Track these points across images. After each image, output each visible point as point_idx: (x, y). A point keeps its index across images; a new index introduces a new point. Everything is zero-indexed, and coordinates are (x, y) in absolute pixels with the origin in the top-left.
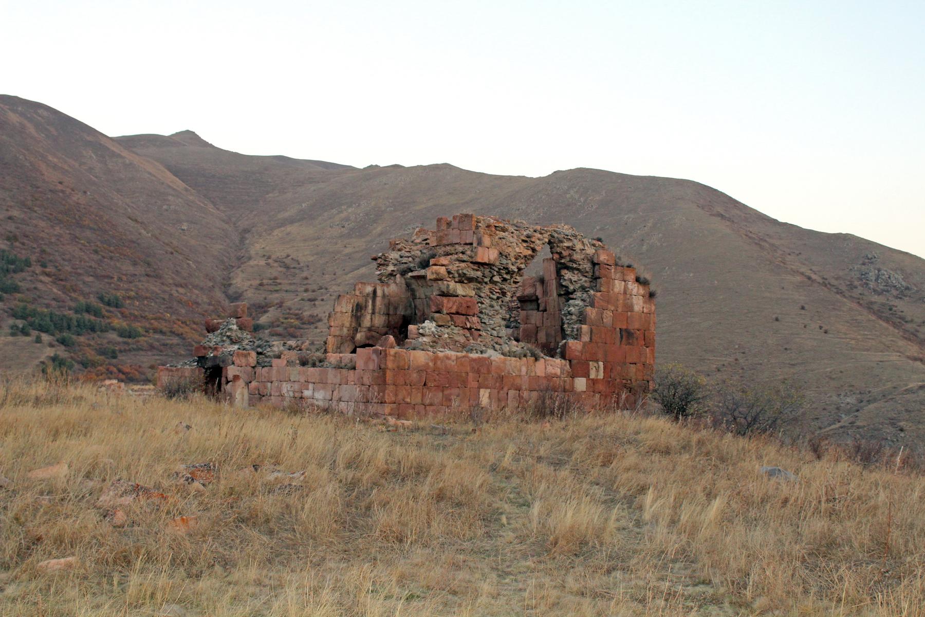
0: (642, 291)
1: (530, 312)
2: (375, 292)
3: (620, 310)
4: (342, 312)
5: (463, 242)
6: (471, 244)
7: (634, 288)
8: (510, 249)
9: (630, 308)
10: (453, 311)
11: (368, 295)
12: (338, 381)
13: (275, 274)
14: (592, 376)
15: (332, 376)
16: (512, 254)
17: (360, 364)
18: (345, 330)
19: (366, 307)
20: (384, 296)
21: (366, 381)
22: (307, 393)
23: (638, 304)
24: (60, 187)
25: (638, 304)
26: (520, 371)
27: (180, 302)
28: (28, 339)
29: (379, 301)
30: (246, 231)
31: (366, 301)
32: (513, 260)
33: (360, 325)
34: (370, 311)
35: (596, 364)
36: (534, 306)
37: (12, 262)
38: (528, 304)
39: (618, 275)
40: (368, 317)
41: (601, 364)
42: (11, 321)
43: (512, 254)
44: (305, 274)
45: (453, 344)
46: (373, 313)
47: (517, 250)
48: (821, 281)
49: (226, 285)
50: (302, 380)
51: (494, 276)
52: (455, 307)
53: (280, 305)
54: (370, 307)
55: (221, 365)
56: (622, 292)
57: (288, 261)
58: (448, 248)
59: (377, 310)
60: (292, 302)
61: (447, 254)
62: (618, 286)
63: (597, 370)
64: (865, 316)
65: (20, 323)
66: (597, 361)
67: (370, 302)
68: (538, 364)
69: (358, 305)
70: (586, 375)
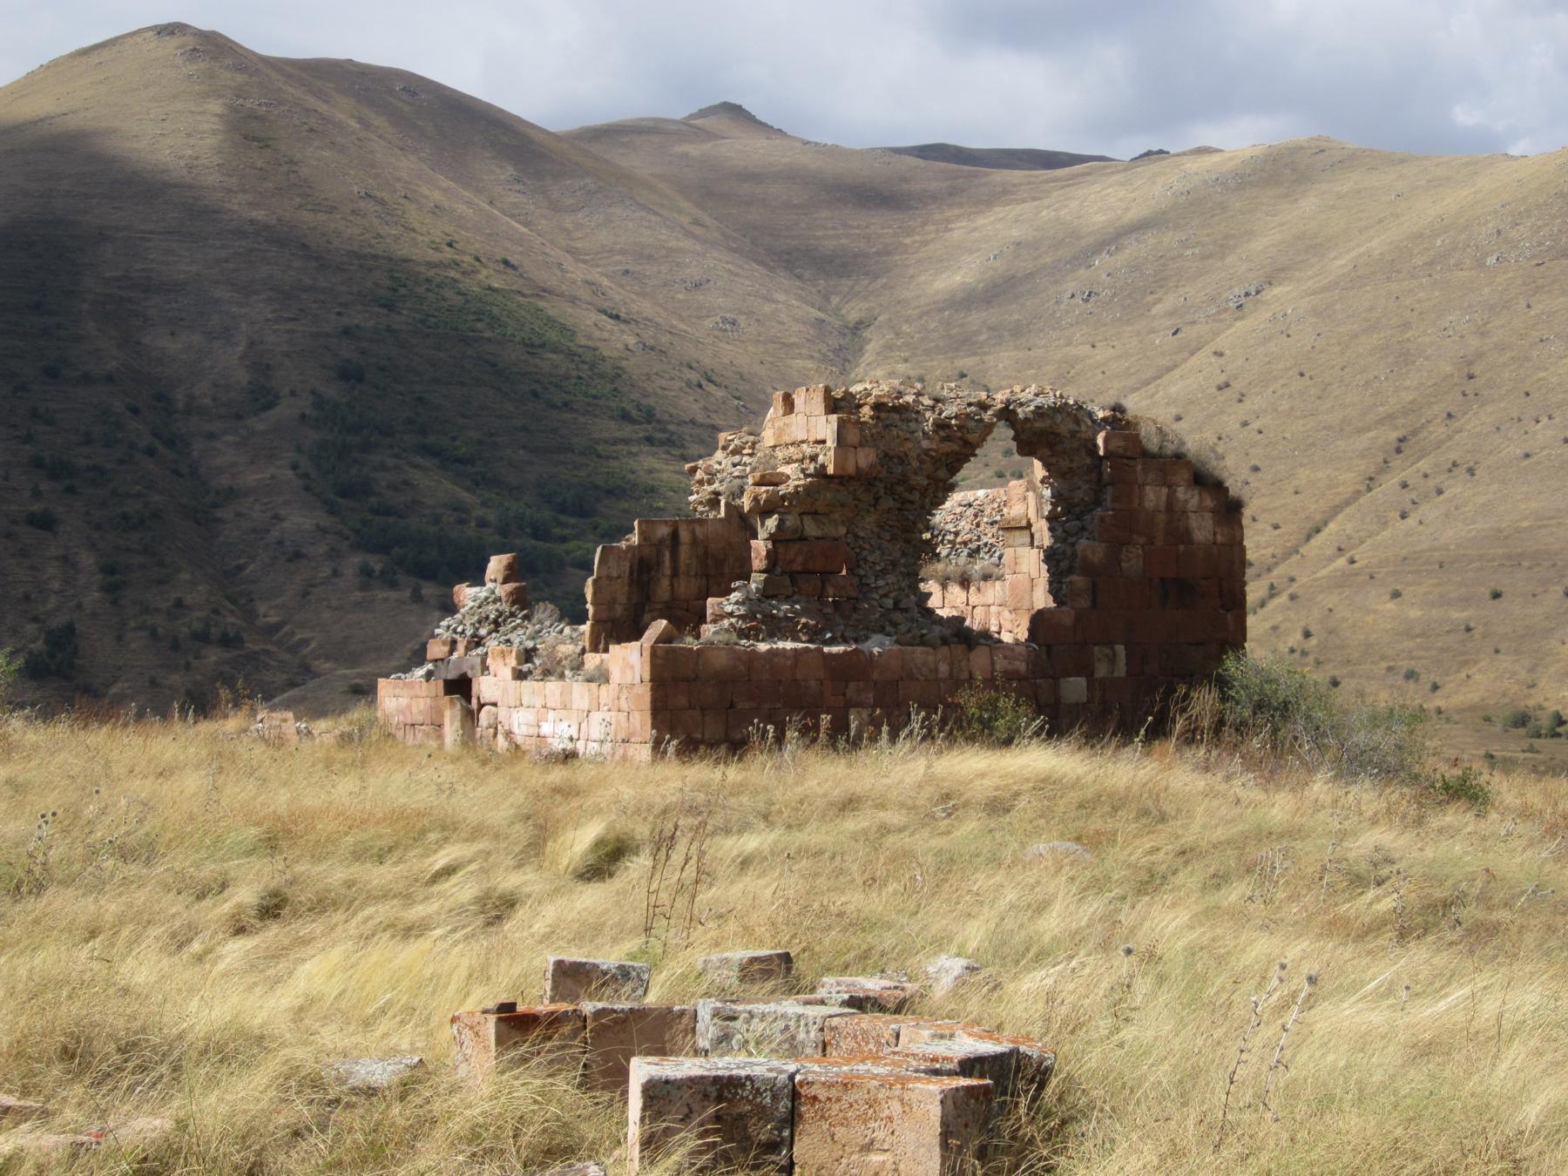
0: (1209, 503)
1: (1020, 550)
2: (675, 535)
3: (1159, 542)
4: (609, 578)
5: (812, 439)
6: (824, 442)
7: (1188, 497)
8: (909, 445)
9: (1185, 536)
10: (797, 567)
11: (661, 541)
12: (585, 705)
14: (1101, 671)
15: (579, 692)
16: (914, 454)
17: (616, 676)
18: (619, 609)
19: (659, 563)
20: (695, 541)
21: (624, 705)
22: (546, 729)
24: (448, 254)
26: (936, 670)
28: (394, 595)
29: (684, 552)
31: (659, 554)
32: (915, 464)
33: (648, 598)
34: (668, 572)
35: (1107, 651)
36: (1024, 537)
38: (1017, 533)
39: (1151, 476)
40: (665, 583)
41: (1120, 649)
42: (356, 559)
43: (914, 454)
46: (675, 574)
47: (925, 444)
50: (539, 702)
51: (877, 499)
52: (800, 559)
54: (667, 563)
55: (470, 674)
56: (1162, 508)
58: (792, 449)
59: (682, 568)
61: (789, 461)
62: (1153, 497)
63: (1112, 660)
65: (376, 563)
66: (1110, 644)
67: (667, 554)
68: (973, 655)
69: (641, 560)
70: (1086, 670)
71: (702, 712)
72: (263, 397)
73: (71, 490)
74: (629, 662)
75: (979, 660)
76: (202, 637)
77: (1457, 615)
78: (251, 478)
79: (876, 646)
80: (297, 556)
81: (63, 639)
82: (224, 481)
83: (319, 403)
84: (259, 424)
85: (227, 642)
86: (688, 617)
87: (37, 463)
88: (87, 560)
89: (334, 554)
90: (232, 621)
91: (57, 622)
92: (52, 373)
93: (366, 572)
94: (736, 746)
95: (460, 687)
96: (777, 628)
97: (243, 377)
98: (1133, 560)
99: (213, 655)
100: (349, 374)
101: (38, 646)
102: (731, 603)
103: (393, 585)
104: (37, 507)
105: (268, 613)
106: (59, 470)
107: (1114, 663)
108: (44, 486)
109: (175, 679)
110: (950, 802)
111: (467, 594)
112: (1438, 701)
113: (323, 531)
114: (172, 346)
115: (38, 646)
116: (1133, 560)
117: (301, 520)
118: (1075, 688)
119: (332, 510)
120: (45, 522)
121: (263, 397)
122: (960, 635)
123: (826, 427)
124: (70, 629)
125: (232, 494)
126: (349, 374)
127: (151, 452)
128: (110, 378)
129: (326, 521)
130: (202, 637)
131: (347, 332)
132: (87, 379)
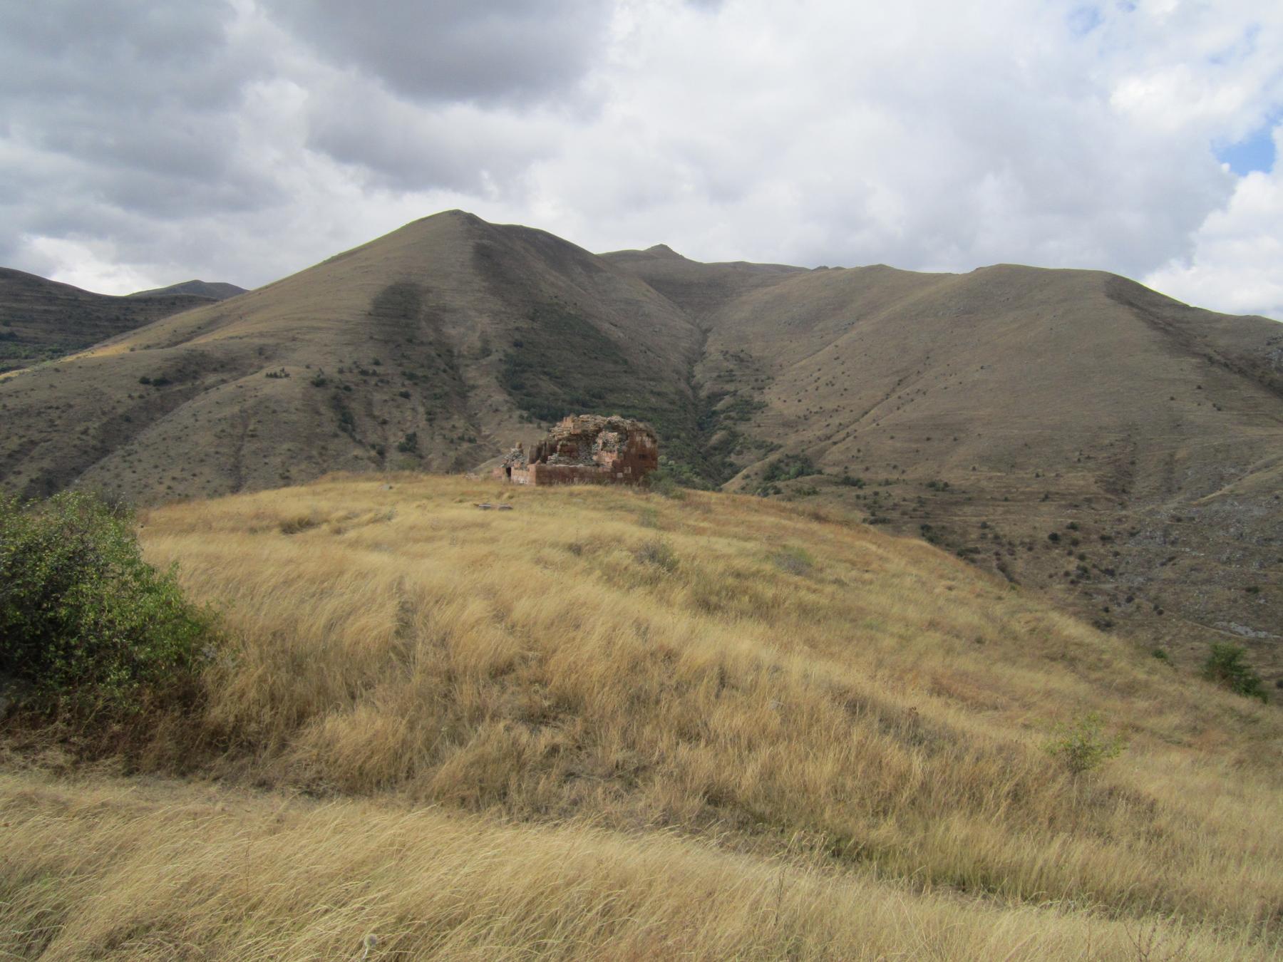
7: (646, 439)
13: (731, 367)
23: (649, 444)
24: (555, 301)
25: (649, 444)
27: (652, 392)
37: (519, 365)
42: (518, 413)
44: (757, 366)
45: (564, 462)
48: (1223, 361)
49: (691, 376)
53: (734, 393)
57: (742, 355)
60: (745, 390)
62: (638, 439)
64: (1260, 395)
65: (525, 414)
71: (545, 478)
72: (486, 352)
73: (416, 384)
74: (532, 467)
75: (600, 470)
76: (461, 439)
77: (914, 446)
78: (481, 382)
79: (581, 465)
80: (497, 410)
81: (412, 438)
82: (471, 382)
83: (506, 355)
84: (484, 362)
85: (470, 441)
86: (544, 460)
87: (404, 374)
88: (421, 410)
89: (510, 410)
90: (472, 433)
91: (410, 431)
92: (410, 341)
93: (521, 417)
94: (551, 484)
95: (509, 471)
96: (560, 462)
97: (479, 344)
99: (465, 445)
100: (517, 344)
101: (403, 440)
104: (403, 390)
105: (486, 431)
106: (411, 377)
108: (407, 382)
109: (452, 454)
110: (571, 494)
112: (904, 477)
113: (507, 402)
114: (453, 332)
115: (403, 440)
116: (633, 450)
117: (499, 397)
118: (620, 475)
119: (510, 394)
120: (406, 396)
121: (486, 352)
123: (571, 425)
124: (415, 435)
125: (473, 387)
126: (517, 344)
127: (445, 371)
128: (430, 343)
129: (508, 398)
130: (461, 439)
131: (517, 329)
132: (422, 343)
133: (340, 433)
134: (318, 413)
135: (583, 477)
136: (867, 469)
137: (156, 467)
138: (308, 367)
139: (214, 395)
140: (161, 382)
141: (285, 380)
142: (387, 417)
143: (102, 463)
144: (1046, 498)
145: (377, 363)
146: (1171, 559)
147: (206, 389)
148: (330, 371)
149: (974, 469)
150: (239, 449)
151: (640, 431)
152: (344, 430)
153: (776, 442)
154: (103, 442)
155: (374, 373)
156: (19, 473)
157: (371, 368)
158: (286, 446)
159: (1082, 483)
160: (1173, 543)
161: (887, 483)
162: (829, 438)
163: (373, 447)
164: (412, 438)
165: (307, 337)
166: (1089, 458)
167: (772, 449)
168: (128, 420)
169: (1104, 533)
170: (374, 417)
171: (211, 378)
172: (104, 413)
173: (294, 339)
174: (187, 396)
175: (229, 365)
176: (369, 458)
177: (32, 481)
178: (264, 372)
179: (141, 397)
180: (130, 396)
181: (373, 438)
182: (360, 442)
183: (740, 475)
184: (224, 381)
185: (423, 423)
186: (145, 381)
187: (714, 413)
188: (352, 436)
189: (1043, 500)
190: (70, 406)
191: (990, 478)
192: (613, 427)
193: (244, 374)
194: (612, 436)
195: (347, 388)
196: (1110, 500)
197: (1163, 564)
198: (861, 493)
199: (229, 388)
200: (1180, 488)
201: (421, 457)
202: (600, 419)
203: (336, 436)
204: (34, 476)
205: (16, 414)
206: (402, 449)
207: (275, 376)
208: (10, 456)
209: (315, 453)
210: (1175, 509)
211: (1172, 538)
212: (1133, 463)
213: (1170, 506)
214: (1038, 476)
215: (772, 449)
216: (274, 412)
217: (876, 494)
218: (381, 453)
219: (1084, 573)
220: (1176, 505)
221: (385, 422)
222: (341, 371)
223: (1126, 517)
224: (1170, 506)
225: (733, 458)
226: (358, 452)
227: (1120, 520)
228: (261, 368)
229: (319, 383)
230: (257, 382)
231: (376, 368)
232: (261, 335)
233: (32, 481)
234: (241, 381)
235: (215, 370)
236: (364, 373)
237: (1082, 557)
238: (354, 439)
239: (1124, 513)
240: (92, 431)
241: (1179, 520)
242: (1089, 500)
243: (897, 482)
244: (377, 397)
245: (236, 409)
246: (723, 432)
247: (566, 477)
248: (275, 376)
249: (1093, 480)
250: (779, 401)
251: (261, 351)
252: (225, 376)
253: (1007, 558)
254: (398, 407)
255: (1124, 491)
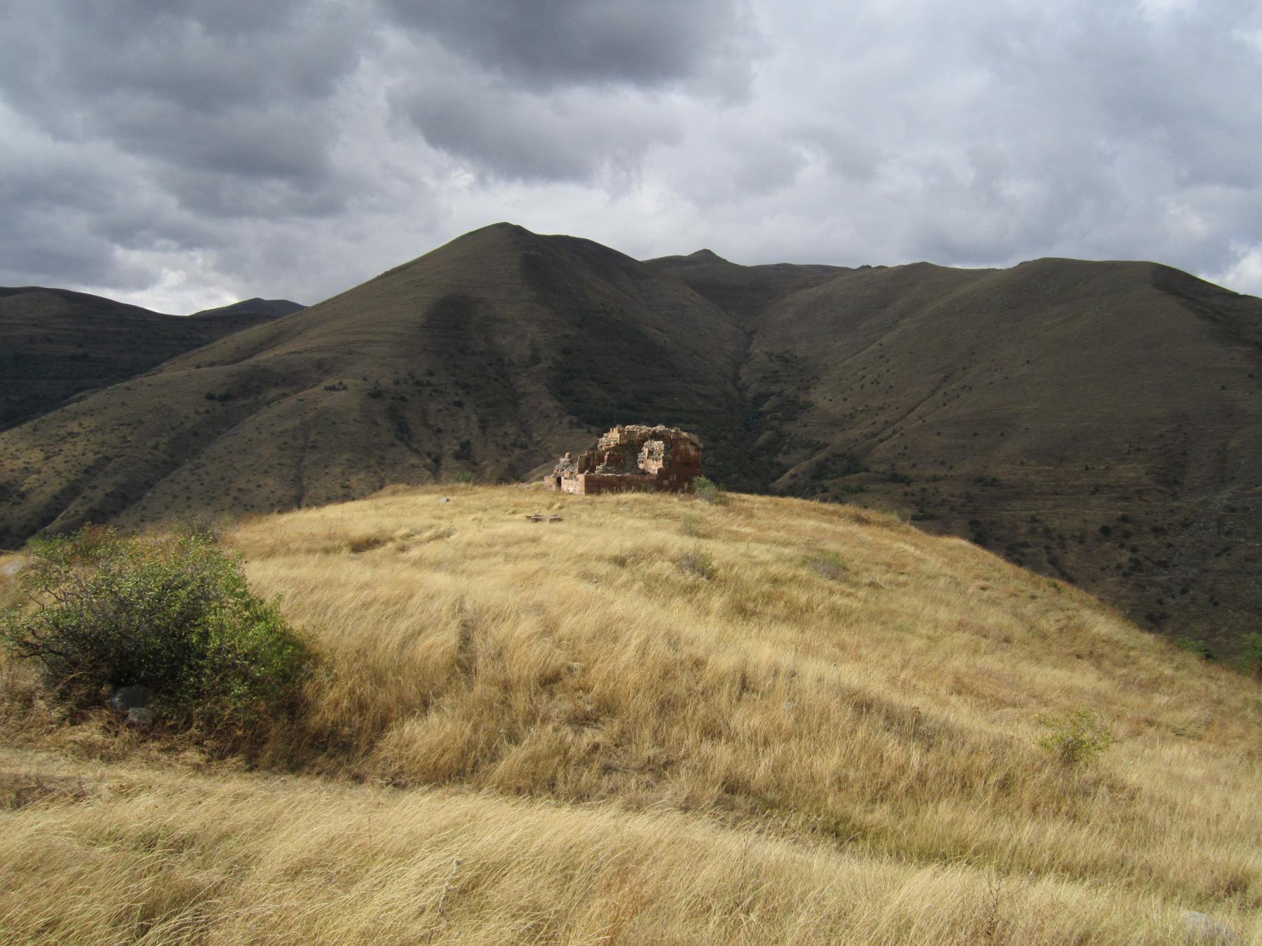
7: (689, 447)
13: (776, 368)
27: (698, 394)
30: (753, 332)
42: (568, 418)
49: (736, 378)
53: (780, 394)
57: (787, 356)
62: (682, 447)
65: (575, 419)
71: (593, 487)
72: (535, 360)
74: (581, 477)
75: (647, 477)
76: (514, 445)
77: (961, 441)
79: (628, 474)
80: (548, 416)
81: (466, 446)
82: (522, 390)
85: (522, 447)
86: (593, 470)
87: (457, 383)
88: (474, 418)
89: (560, 416)
91: (463, 440)
93: (571, 422)
94: (599, 493)
95: (559, 481)
96: (608, 471)
97: (529, 353)
98: (678, 459)
99: (518, 452)
100: (566, 352)
101: (457, 448)
102: (600, 467)
103: (581, 427)
104: (457, 399)
106: (464, 386)
107: (674, 478)
108: (460, 392)
109: (505, 460)
110: (618, 503)
111: (562, 460)
115: (457, 448)
116: (678, 459)
117: (549, 404)
118: (666, 482)
120: (460, 404)
121: (535, 360)
122: (644, 472)
123: (618, 436)
124: (468, 442)
125: (524, 395)
126: (566, 352)
127: (496, 380)
128: (481, 353)
130: (514, 445)
131: (566, 336)
133: (397, 443)
134: (376, 423)
135: (630, 485)
136: (914, 465)
137: (222, 479)
138: (365, 379)
139: (276, 409)
140: (225, 398)
141: (343, 393)
142: (441, 425)
143: (171, 476)
144: (1096, 490)
145: (431, 374)
146: (1226, 550)
147: (269, 403)
148: (386, 382)
149: (1022, 463)
150: (301, 460)
151: (685, 440)
152: (401, 439)
153: (823, 440)
154: (172, 456)
155: (429, 384)
156: (95, 487)
157: (425, 379)
158: (345, 456)
159: (1132, 474)
160: (1228, 534)
161: (935, 479)
162: (874, 435)
163: (429, 455)
164: (466, 446)
165: (363, 350)
166: (1139, 449)
167: (819, 447)
168: (196, 434)
169: (1155, 524)
170: (429, 426)
171: (273, 393)
172: (173, 429)
173: (351, 353)
174: (252, 410)
175: (291, 379)
176: (425, 466)
177: (107, 495)
178: (324, 384)
179: (207, 412)
180: (197, 412)
181: (429, 446)
182: (416, 451)
183: (787, 475)
184: (285, 395)
185: (476, 431)
186: (210, 397)
187: (761, 414)
188: (408, 445)
189: (1093, 493)
190: (141, 423)
191: (1039, 472)
192: (656, 436)
193: (304, 388)
194: (658, 445)
195: (403, 399)
196: (1160, 491)
197: (1217, 555)
198: (908, 489)
199: (292, 401)
200: (1233, 478)
201: (475, 464)
202: (645, 429)
203: (393, 445)
204: (109, 490)
205: (91, 431)
206: (457, 456)
207: (333, 388)
208: (86, 472)
209: (373, 462)
210: (1229, 499)
211: (1226, 529)
212: (1184, 454)
213: (1224, 497)
214: (1087, 469)
215: (819, 447)
216: (334, 423)
217: (924, 490)
218: (437, 461)
219: (1136, 565)
220: (1229, 495)
221: (439, 431)
222: (397, 383)
223: (1178, 508)
224: (1224, 497)
225: (780, 458)
226: (414, 460)
227: (1172, 511)
228: (320, 381)
229: (376, 394)
230: (319, 397)
231: (429, 378)
232: (320, 349)
233: (107, 495)
234: (301, 395)
235: (277, 384)
236: (418, 383)
237: (1134, 550)
238: (411, 448)
239: (1176, 504)
240: (162, 446)
241: (1233, 510)
242: (1139, 492)
243: (945, 478)
244: (433, 407)
245: (297, 422)
246: (770, 433)
247: (615, 486)
248: (333, 388)
249: (1143, 471)
250: (823, 399)
251: (319, 364)
252: (286, 390)
253: (1058, 552)
254: (452, 415)
255: (1176, 482)
